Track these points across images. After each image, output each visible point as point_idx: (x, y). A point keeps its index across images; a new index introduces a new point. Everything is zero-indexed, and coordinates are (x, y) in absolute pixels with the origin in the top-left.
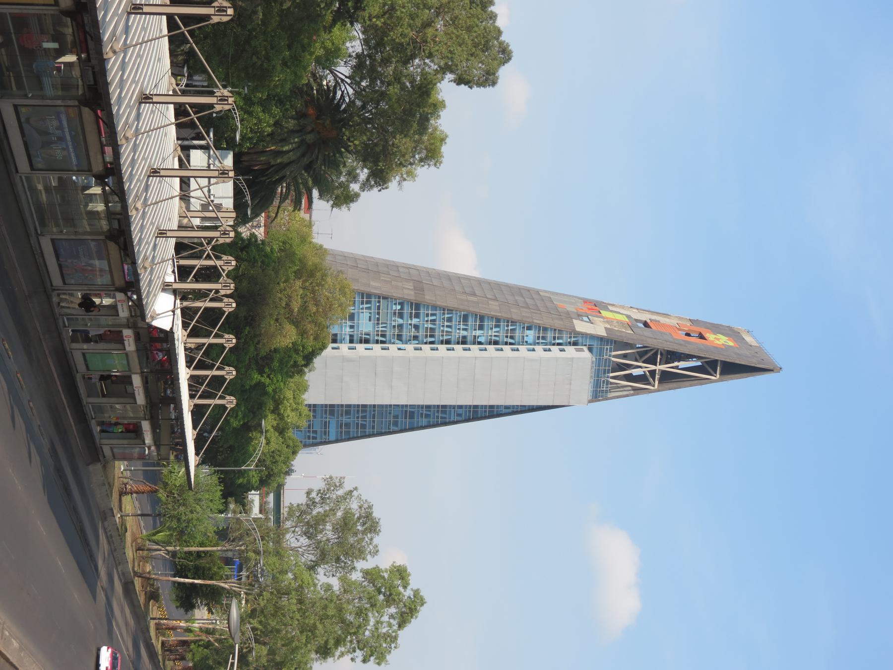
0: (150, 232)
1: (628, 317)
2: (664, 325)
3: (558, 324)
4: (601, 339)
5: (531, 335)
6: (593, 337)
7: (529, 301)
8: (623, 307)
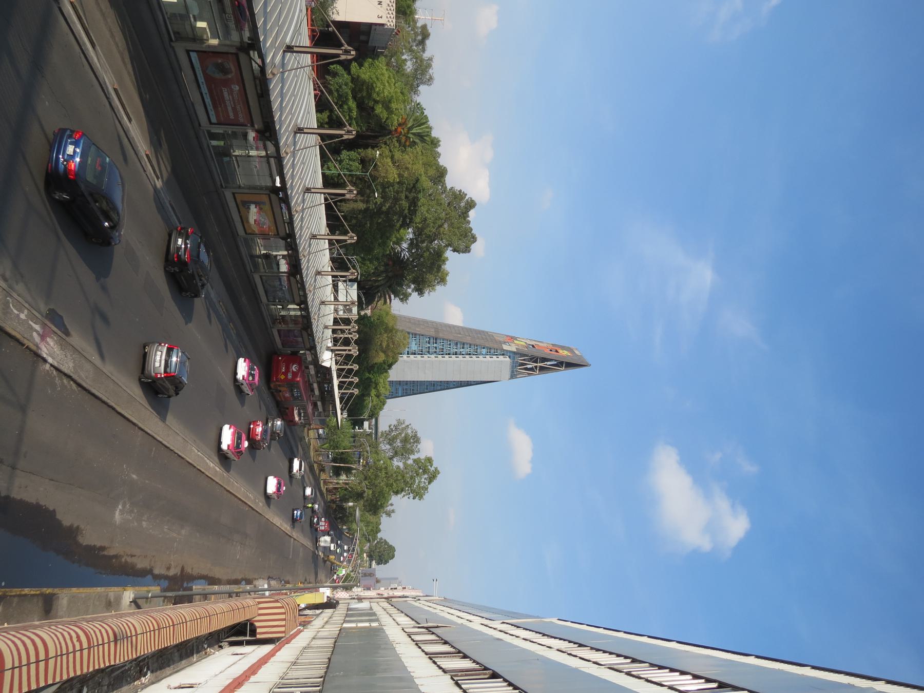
0: (321, 327)
3: (496, 346)
4: (514, 353)
5: (484, 351)
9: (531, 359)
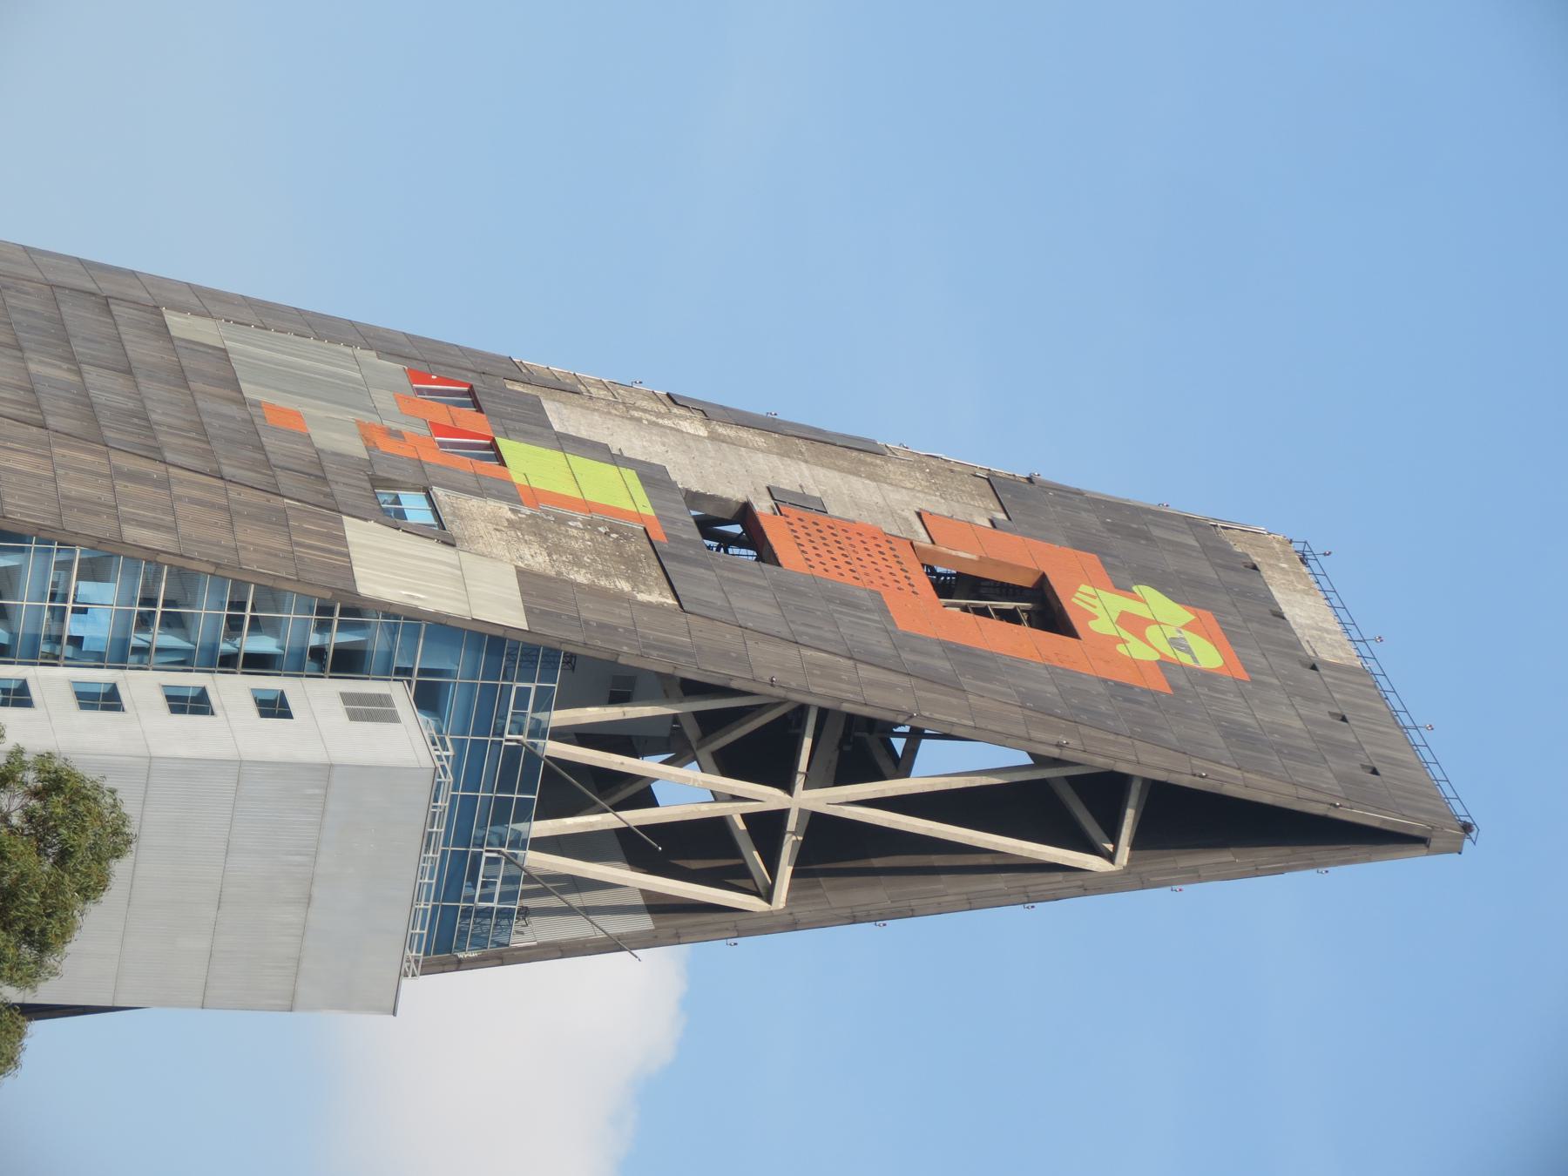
1: (653, 478)
3: (258, 549)
4: (493, 645)
6: (444, 630)
7: (106, 388)
8: (618, 399)
9: (710, 723)
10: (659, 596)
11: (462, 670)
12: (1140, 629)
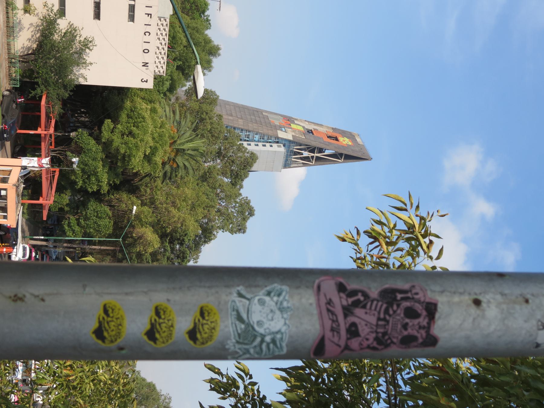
1: (304, 127)
2: (320, 132)
3: (270, 133)
4: (290, 141)
5: (257, 137)
6: (286, 140)
7: (258, 119)
9: (308, 148)
10: (304, 137)
11: (287, 143)
12: (345, 141)
